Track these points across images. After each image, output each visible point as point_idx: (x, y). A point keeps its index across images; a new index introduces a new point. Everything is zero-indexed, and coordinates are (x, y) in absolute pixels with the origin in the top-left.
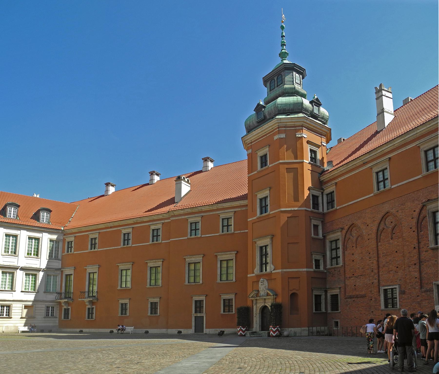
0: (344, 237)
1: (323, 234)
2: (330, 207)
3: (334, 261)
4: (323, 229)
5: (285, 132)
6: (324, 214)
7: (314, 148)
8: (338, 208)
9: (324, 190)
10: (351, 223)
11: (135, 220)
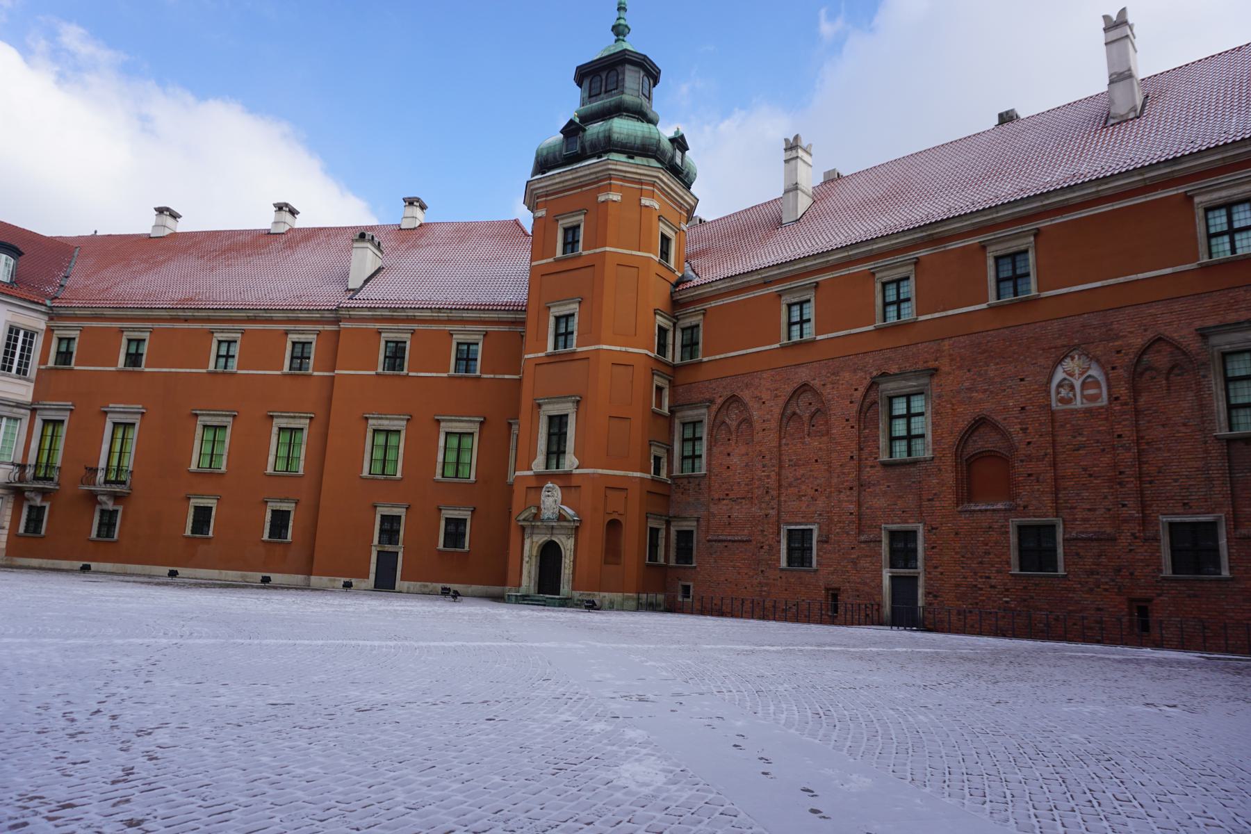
0: (712, 418)
2: (687, 355)
3: (688, 463)
4: (671, 396)
5: (620, 189)
6: (675, 368)
8: (705, 359)
10: (729, 394)
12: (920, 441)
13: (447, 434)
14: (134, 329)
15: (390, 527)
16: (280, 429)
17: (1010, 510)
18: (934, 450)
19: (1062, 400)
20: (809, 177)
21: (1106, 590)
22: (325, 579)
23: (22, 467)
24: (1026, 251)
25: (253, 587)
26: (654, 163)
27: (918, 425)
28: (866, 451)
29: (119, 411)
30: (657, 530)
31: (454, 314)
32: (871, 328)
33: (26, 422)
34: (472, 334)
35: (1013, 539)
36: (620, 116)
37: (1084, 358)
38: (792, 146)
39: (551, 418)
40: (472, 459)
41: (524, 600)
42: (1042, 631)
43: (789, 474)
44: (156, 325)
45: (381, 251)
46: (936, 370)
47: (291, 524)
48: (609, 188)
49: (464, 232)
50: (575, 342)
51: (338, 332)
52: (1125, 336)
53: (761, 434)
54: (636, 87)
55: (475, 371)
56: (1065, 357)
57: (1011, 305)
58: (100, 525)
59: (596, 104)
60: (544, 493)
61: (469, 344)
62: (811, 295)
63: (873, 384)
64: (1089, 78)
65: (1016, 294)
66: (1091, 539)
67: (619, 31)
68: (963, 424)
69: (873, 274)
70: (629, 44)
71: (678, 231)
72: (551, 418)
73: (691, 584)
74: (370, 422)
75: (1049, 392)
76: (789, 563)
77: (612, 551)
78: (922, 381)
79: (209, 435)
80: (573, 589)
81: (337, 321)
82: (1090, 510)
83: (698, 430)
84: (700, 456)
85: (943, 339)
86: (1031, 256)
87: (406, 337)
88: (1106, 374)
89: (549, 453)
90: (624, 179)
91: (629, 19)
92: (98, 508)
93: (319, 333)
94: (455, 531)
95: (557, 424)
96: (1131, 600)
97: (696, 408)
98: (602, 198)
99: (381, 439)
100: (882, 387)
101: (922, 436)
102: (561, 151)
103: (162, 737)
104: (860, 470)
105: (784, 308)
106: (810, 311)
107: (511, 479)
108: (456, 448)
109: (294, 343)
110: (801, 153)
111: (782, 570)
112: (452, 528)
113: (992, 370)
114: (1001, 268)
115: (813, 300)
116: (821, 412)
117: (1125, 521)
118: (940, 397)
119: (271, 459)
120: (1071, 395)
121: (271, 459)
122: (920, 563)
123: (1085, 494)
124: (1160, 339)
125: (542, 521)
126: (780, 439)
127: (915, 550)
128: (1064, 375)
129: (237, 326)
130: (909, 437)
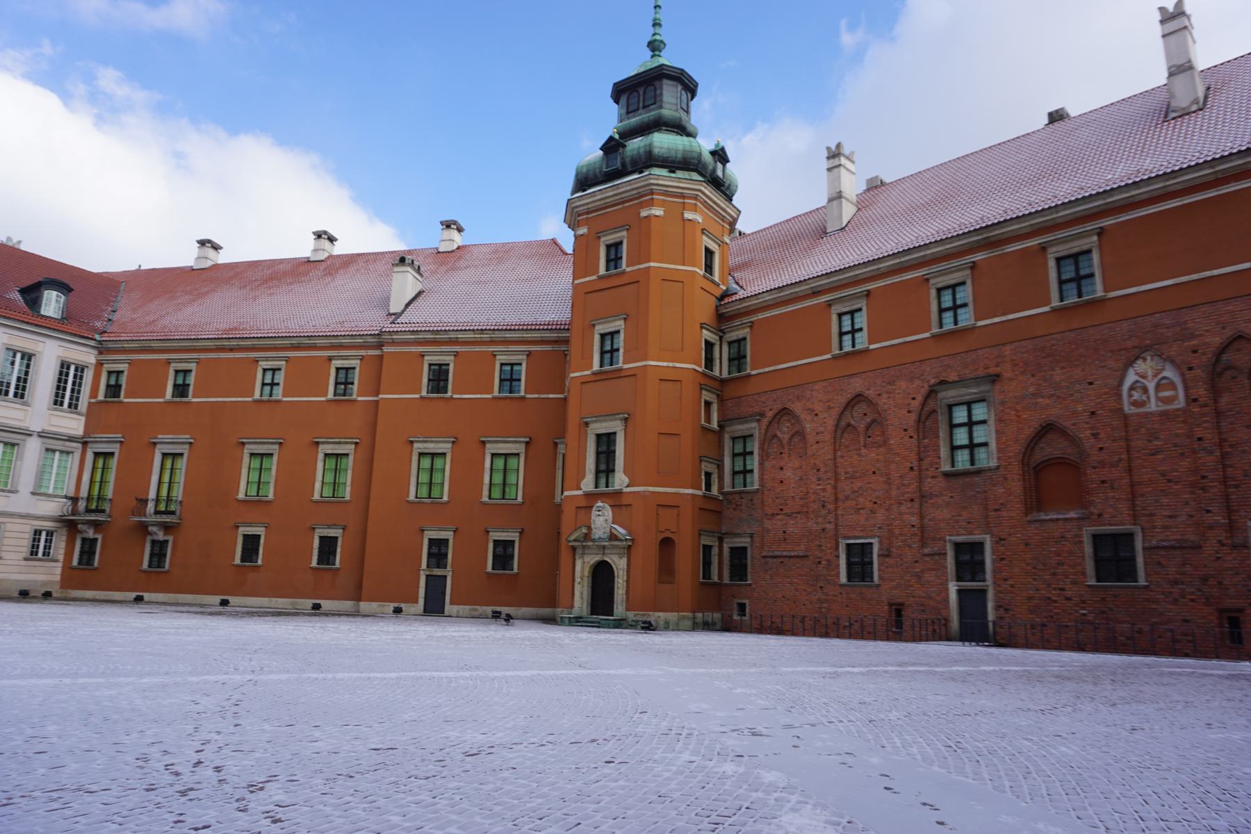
2: (734, 369)
6: (723, 382)
8: (754, 372)
10: (780, 407)
12: (983, 449)
13: (493, 455)
14: (181, 361)
15: (438, 551)
16: (326, 455)
17: (1083, 519)
18: (999, 459)
19: (1135, 404)
20: (852, 185)
21: (1192, 600)
22: (375, 605)
23: (75, 500)
24: (1089, 251)
25: (304, 614)
26: (695, 176)
27: (980, 435)
28: (926, 462)
29: (168, 441)
30: (710, 547)
31: (497, 335)
32: (927, 335)
33: (77, 455)
34: (515, 354)
35: (1088, 549)
36: (659, 130)
37: (1156, 358)
38: (835, 154)
39: (599, 436)
40: (518, 479)
41: (578, 621)
42: (1124, 645)
43: (846, 487)
44: (202, 356)
45: (421, 275)
46: (998, 376)
47: (339, 550)
48: (651, 203)
49: (502, 253)
50: (621, 359)
51: (382, 356)
52: (1200, 335)
53: (815, 446)
54: (674, 101)
55: (519, 391)
56: (1137, 358)
57: (1076, 307)
58: (152, 555)
59: (634, 120)
60: (594, 513)
61: (512, 365)
62: (862, 304)
63: (932, 393)
64: (1150, 72)
65: (1080, 295)
66: (1174, 548)
67: (655, 47)
68: (1029, 431)
69: (927, 280)
70: (665, 59)
71: (722, 244)
72: (599, 436)
73: (747, 602)
74: (416, 445)
75: (1120, 396)
76: (849, 578)
77: (666, 569)
78: (983, 388)
79: (256, 463)
80: (627, 610)
81: (380, 346)
82: (1170, 517)
83: (748, 445)
84: (751, 471)
85: (1004, 344)
86: (1095, 256)
87: (449, 359)
88: (1182, 375)
89: (598, 472)
90: (666, 194)
91: (664, 35)
92: (149, 538)
93: (362, 358)
94: (503, 553)
95: (606, 443)
96: (1221, 611)
97: (747, 422)
98: (644, 213)
99: (426, 463)
100: (941, 395)
101: (985, 444)
102: (601, 168)
103: (275, 793)
104: (920, 480)
105: (834, 318)
106: (861, 320)
107: (558, 499)
108: (502, 469)
109: (338, 369)
110: (843, 161)
111: (842, 586)
112: (500, 550)
113: (1058, 375)
114: (1063, 270)
115: (864, 308)
116: (877, 422)
117: (1211, 528)
118: (1003, 403)
119: (318, 485)
120: (1144, 398)
121: (318, 485)
122: (989, 575)
123: (1165, 501)
124: (1240, 337)
125: (593, 540)
126: (835, 451)
127: (982, 563)
128: (1137, 378)
129: (281, 354)
130: (972, 446)
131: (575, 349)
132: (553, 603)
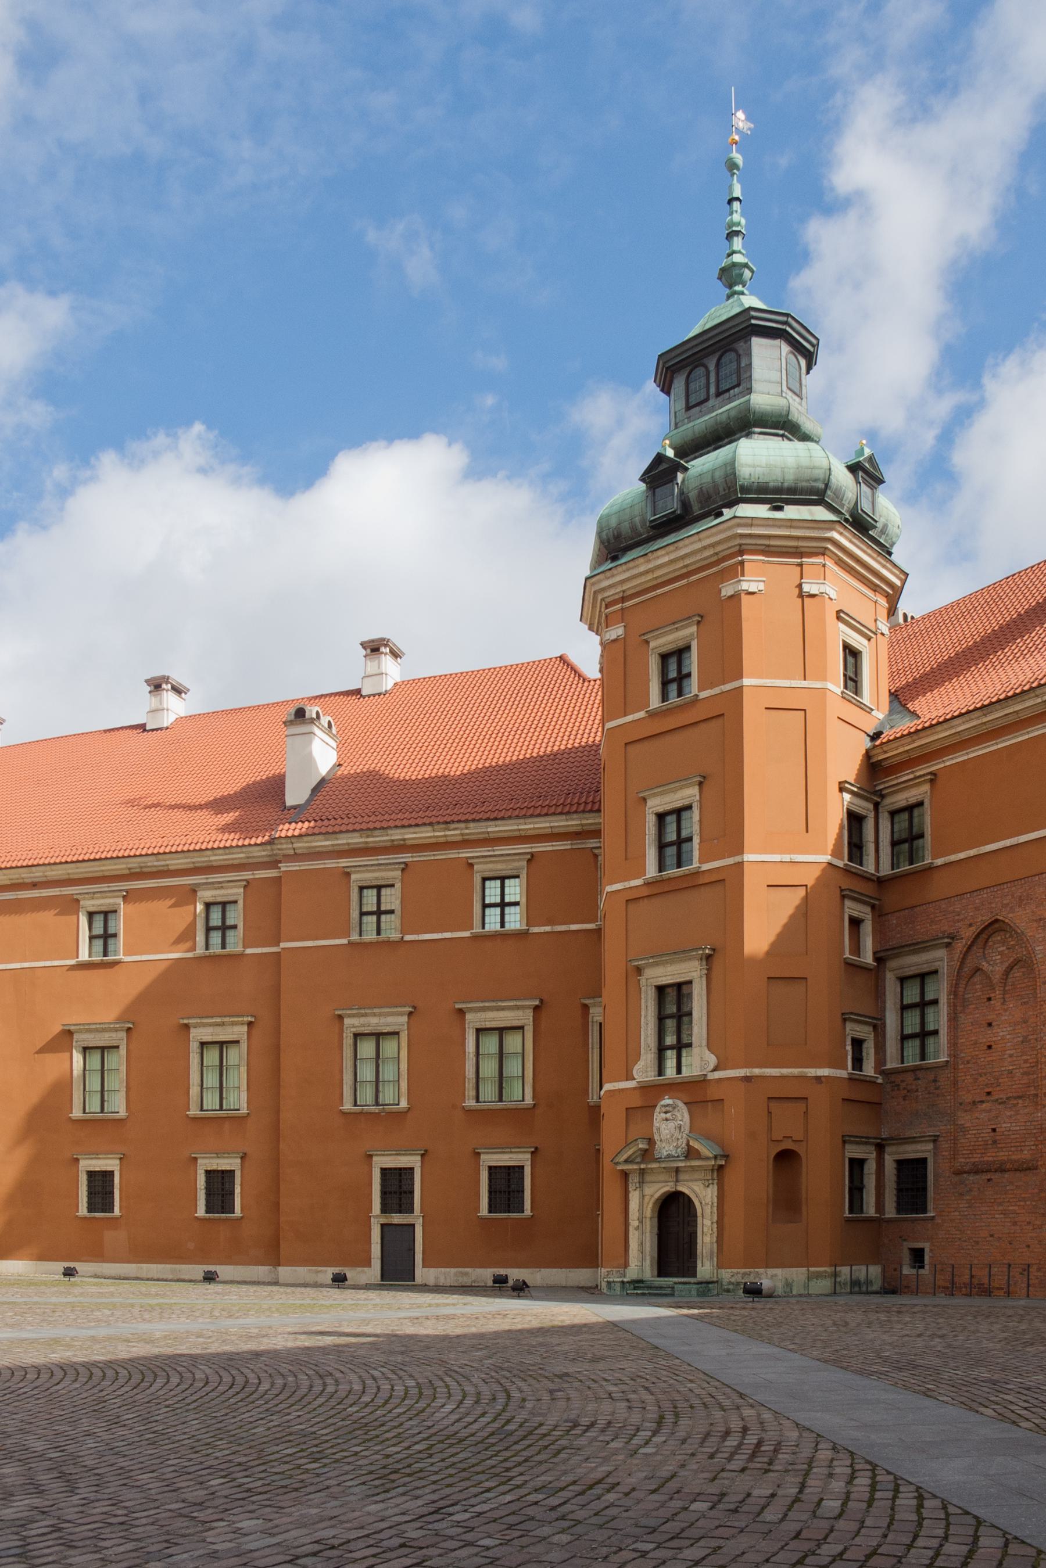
1: (874, 953)
4: (879, 932)
7: (857, 641)
9: (883, 797)
11: (134, 863)
36: (748, 435)
50: (696, 854)
97: (925, 949)
119: (194, 1091)
131: (610, 846)
132: (590, 1257)
